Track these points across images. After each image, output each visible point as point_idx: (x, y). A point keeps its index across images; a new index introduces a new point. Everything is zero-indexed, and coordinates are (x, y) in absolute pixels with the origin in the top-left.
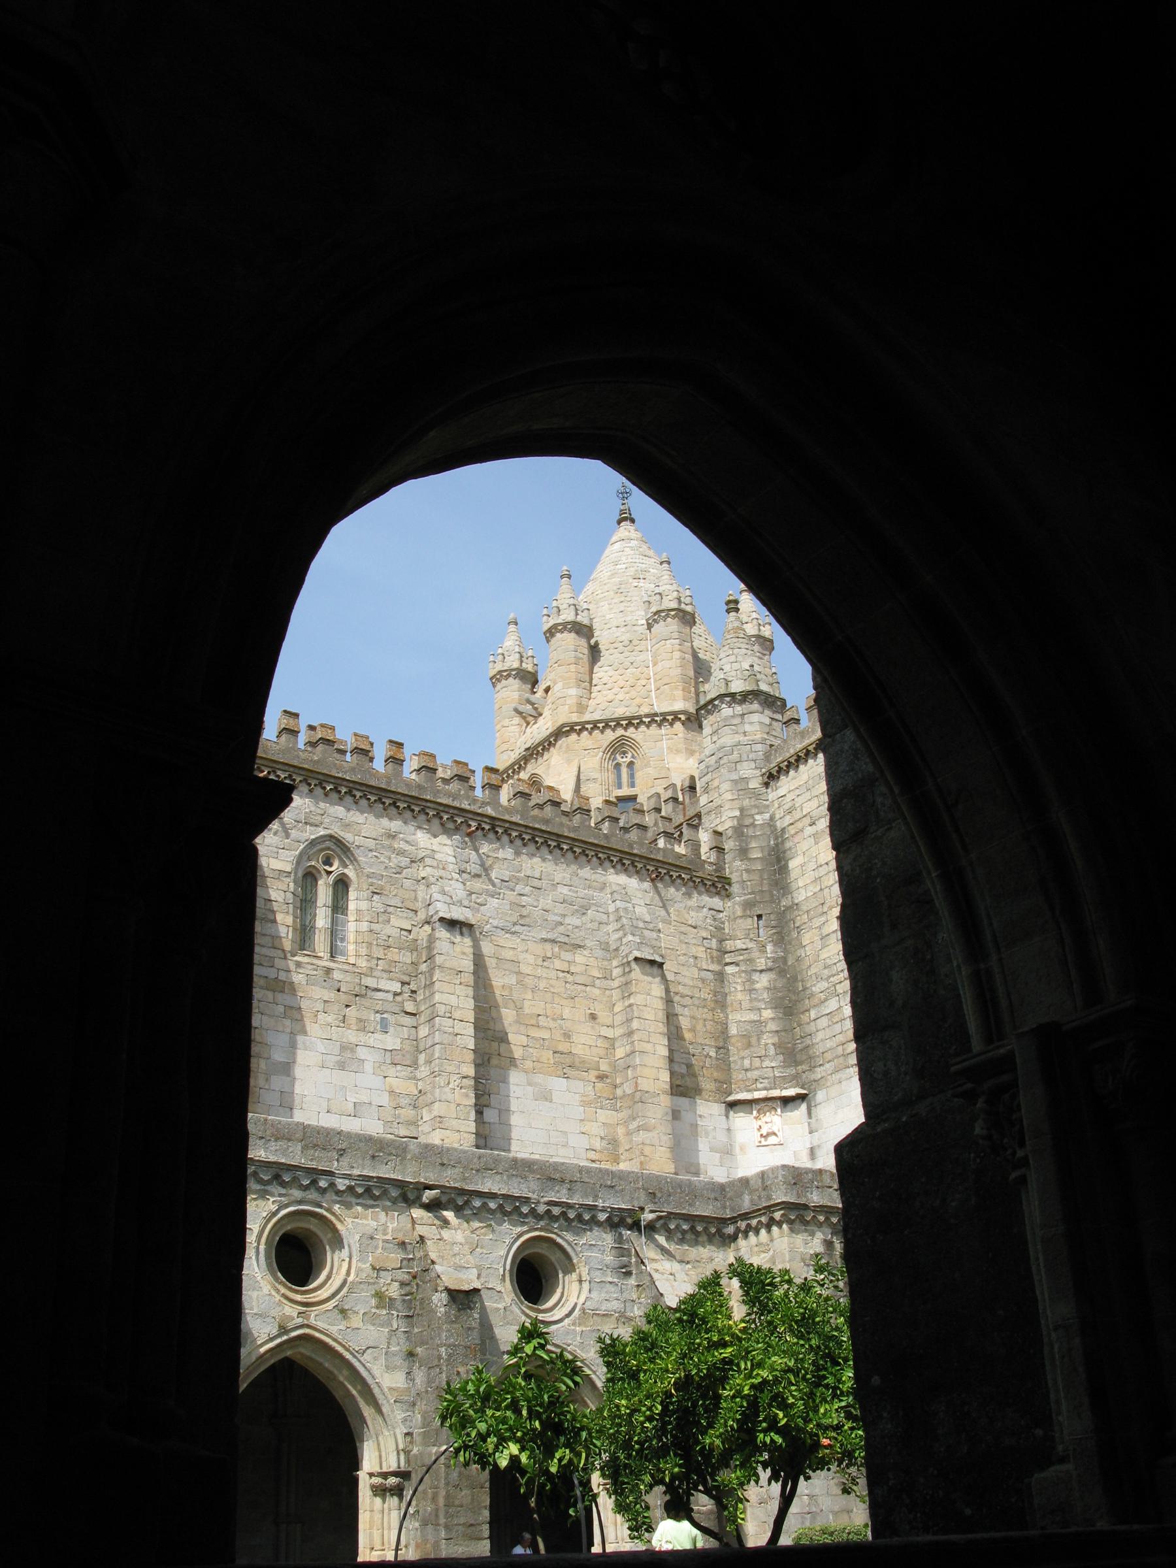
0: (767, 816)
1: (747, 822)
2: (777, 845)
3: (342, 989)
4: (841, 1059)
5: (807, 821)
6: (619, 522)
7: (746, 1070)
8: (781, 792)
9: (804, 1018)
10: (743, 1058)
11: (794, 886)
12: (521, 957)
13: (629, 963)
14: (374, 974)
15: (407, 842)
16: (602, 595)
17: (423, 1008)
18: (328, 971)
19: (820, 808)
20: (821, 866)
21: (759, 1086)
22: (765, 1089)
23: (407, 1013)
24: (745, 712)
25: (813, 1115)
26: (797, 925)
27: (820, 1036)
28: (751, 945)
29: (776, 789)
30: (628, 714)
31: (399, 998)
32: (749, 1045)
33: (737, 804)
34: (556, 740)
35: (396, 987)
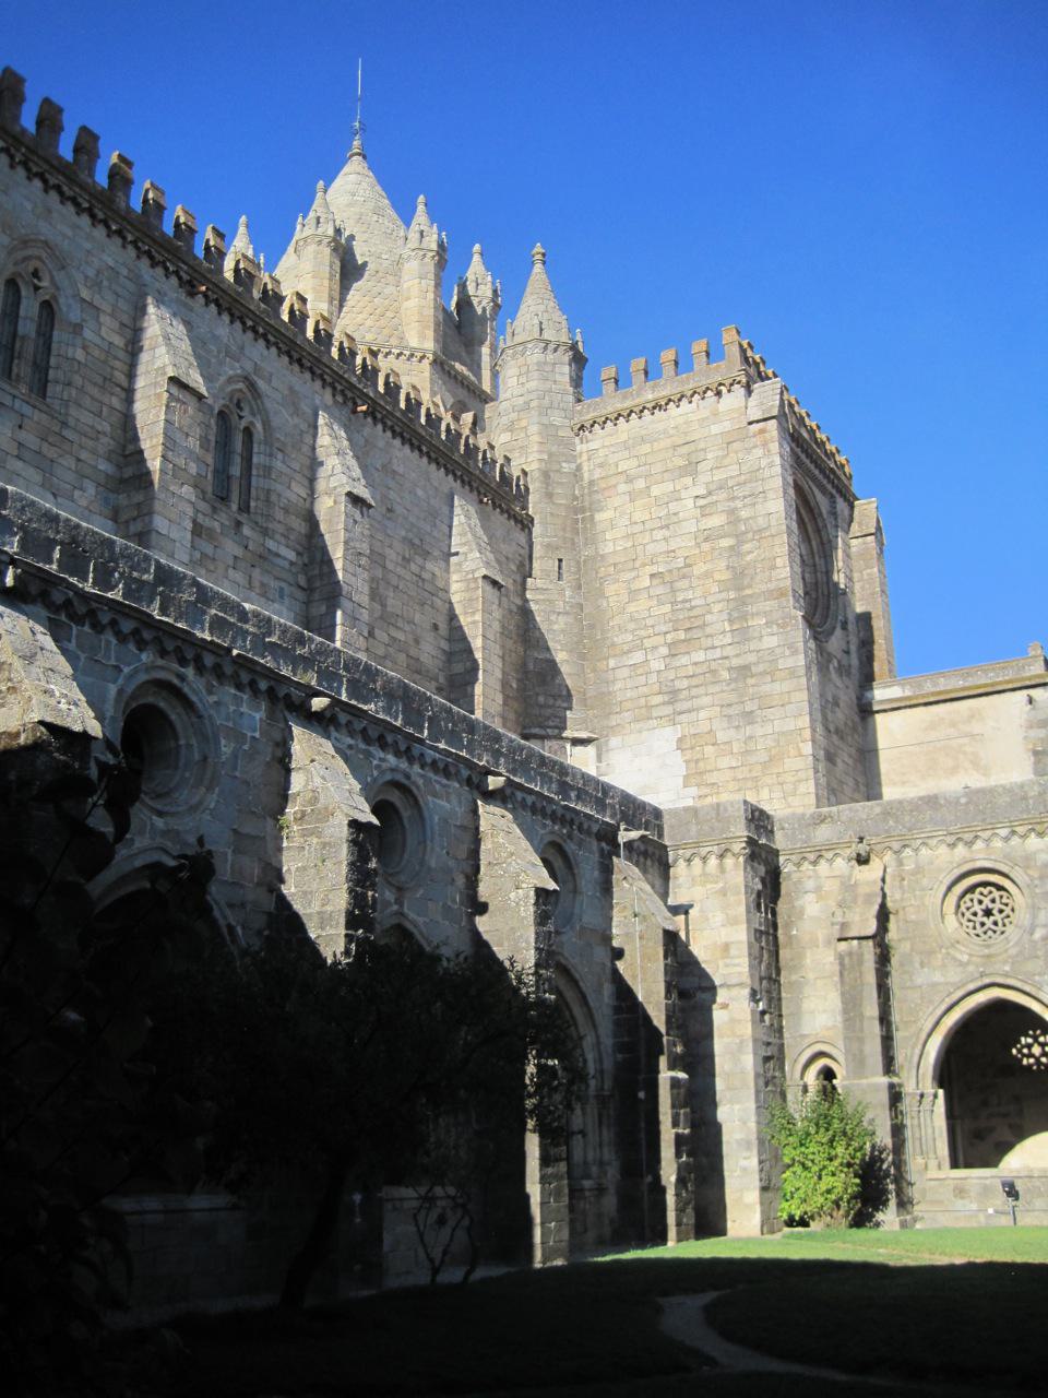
0: (573, 466)
1: (556, 467)
3: (250, 548)
5: (623, 478)
8: (592, 446)
9: (601, 665)
10: (538, 694)
12: (388, 551)
14: (277, 537)
17: (318, 584)
18: (239, 524)
20: (636, 523)
21: (551, 724)
22: (556, 727)
23: (300, 587)
25: (604, 757)
26: (599, 575)
27: (619, 685)
29: (587, 442)
35: (292, 556)
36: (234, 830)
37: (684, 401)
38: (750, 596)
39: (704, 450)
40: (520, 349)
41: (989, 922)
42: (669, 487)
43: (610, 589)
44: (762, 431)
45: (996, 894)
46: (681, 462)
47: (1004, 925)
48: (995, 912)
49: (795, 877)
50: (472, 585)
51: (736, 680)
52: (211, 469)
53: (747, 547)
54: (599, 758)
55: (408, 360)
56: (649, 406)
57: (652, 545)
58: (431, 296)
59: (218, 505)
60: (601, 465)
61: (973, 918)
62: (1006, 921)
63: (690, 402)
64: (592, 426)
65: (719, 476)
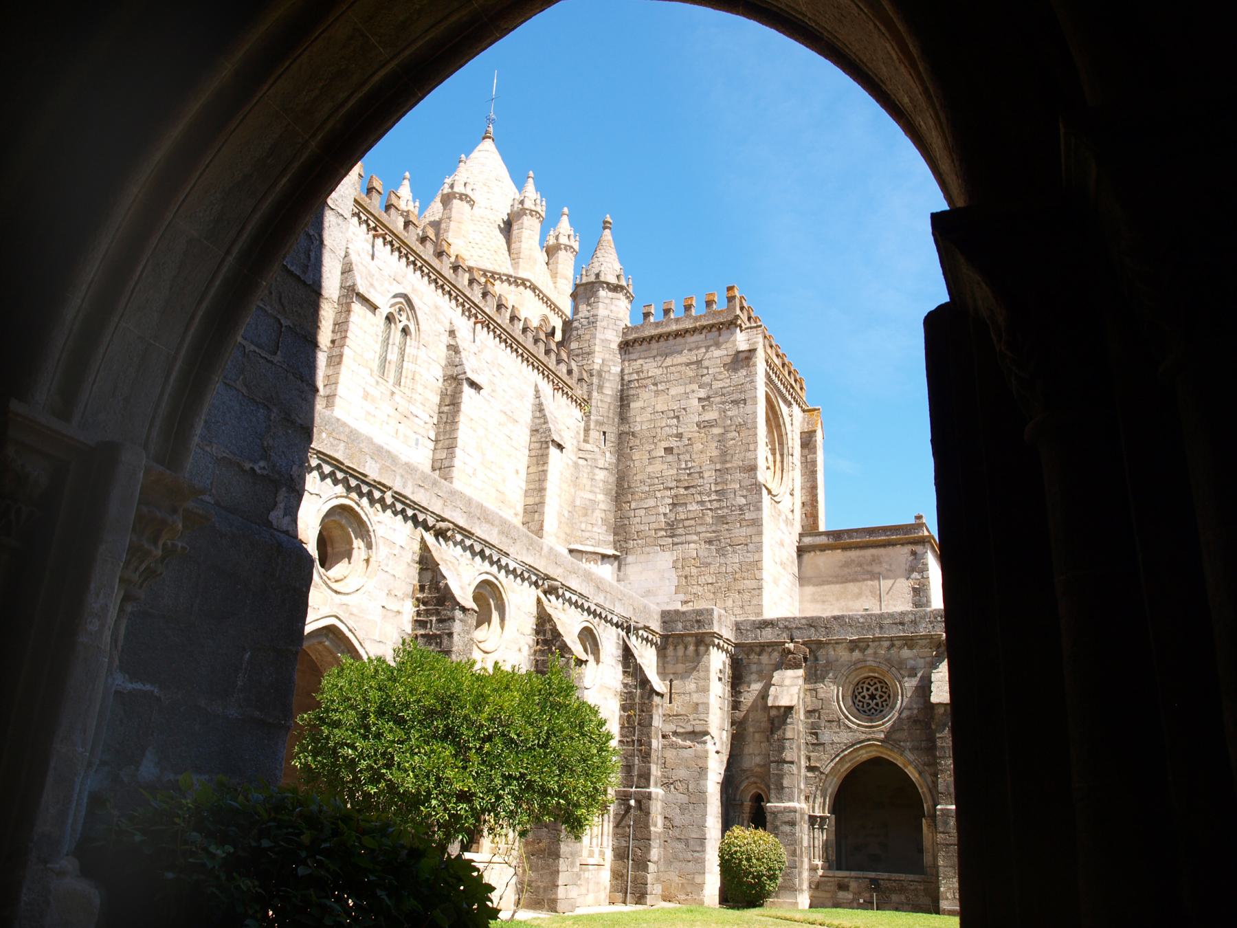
0: (619, 369)
1: (606, 369)
2: (622, 390)
4: (652, 539)
6: (484, 138)
7: (582, 531)
9: (626, 506)
10: (581, 522)
11: (631, 420)
13: (547, 442)
15: (445, 316)
18: (393, 393)
22: (592, 545)
25: (622, 569)
26: (631, 445)
27: (638, 520)
28: (596, 450)
29: (629, 353)
30: (492, 269)
31: (427, 426)
32: (586, 515)
33: (601, 355)
35: (427, 419)
36: (383, 607)
38: (731, 468)
41: (873, 704)
42: (681, 390)
43: (636, 455)
45: (878, 685)
46: (691, 374)
47: (883, 706)
48: (877, 697)
49: (745, 661)
50: (544, 446)
51: (716, 525)
52: (378, 355)
53: (730, 435)
54: (619, 569)
57: (667, 428)
59: (380, 380)
61: (862, 700)
62: (884, 703)
65: (717, 385)
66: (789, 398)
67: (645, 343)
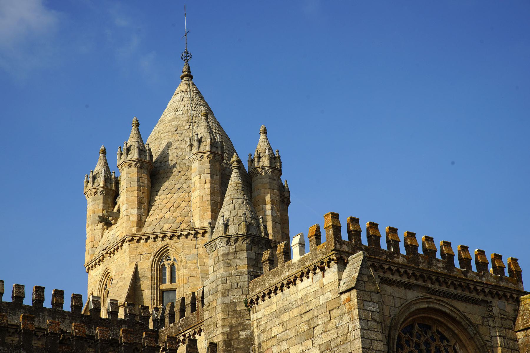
0: (248, 332)
1: (235, 336)
5: (274, 341)
8: (260, 315)
16: (162, 135)
19: (283, 333)
24: (237, 249)
29: (256, 312)
34: (122, 246)
37: (304, 278)
39: (317, 317)
40: (213, 244)
44: (349, 300)
46: (304, 327)
55: (195, 237)
56: (285, 282)
58: (208, 185)
60: (264, 331)
63: (308, 277)
64: (257, 299)
66: (481, 297)
67: (266, 298)
